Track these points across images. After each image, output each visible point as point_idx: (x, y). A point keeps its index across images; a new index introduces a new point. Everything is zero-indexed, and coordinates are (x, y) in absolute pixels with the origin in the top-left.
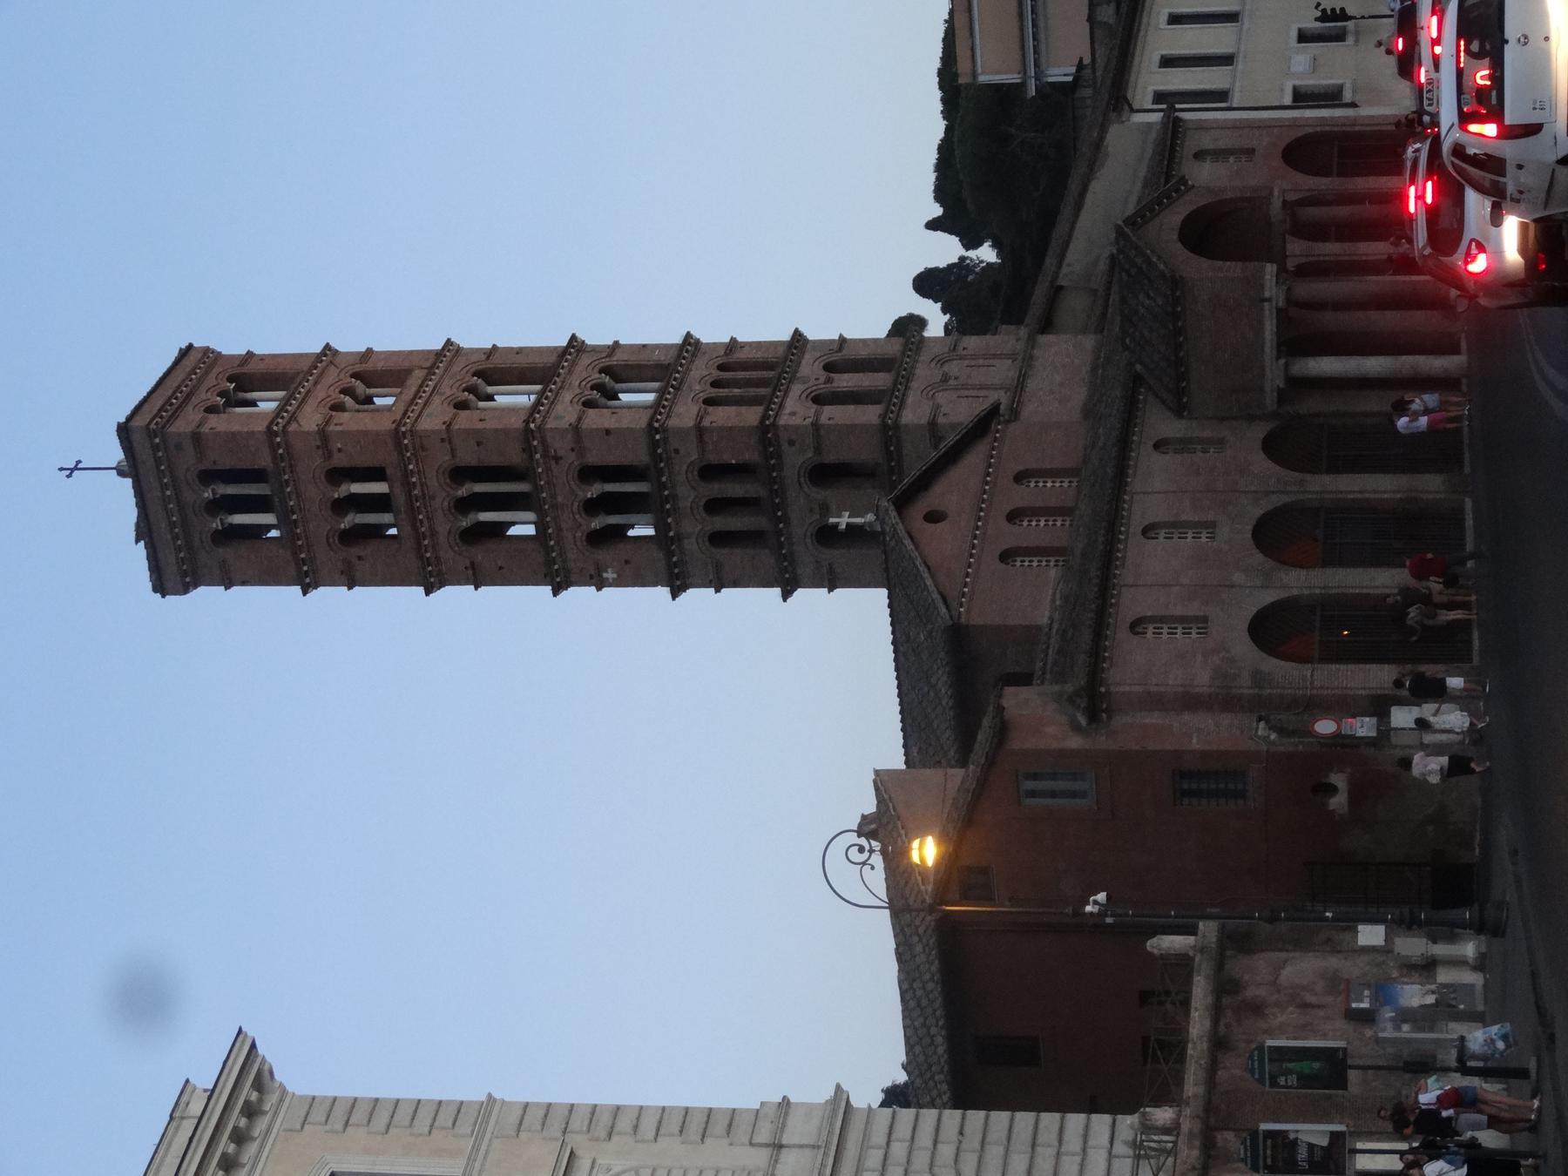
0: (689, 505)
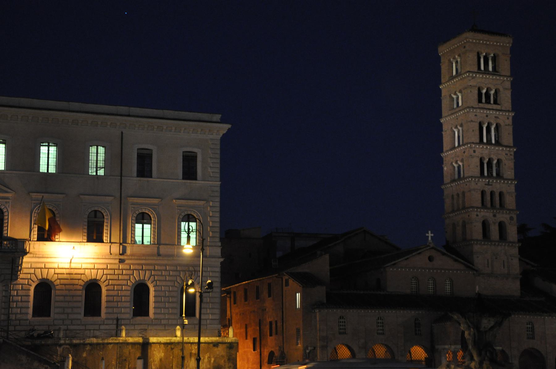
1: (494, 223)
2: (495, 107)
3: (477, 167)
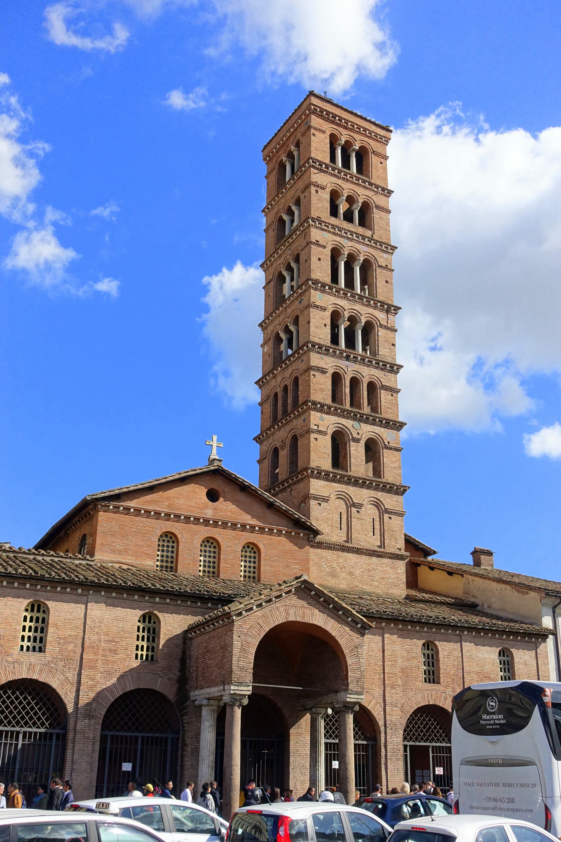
0: (285, 376)
1: (357, 441)
2: (361, 230)
3: (325, 325)
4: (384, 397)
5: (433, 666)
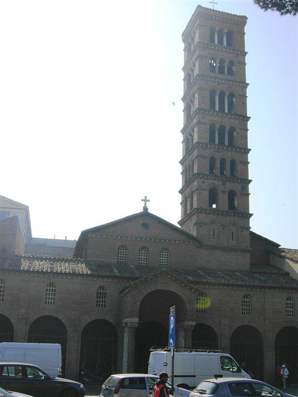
1: (223, 192)
2: (229, 77)
3: (206, 132)
4: (239, 167)
5: (249, 306)
